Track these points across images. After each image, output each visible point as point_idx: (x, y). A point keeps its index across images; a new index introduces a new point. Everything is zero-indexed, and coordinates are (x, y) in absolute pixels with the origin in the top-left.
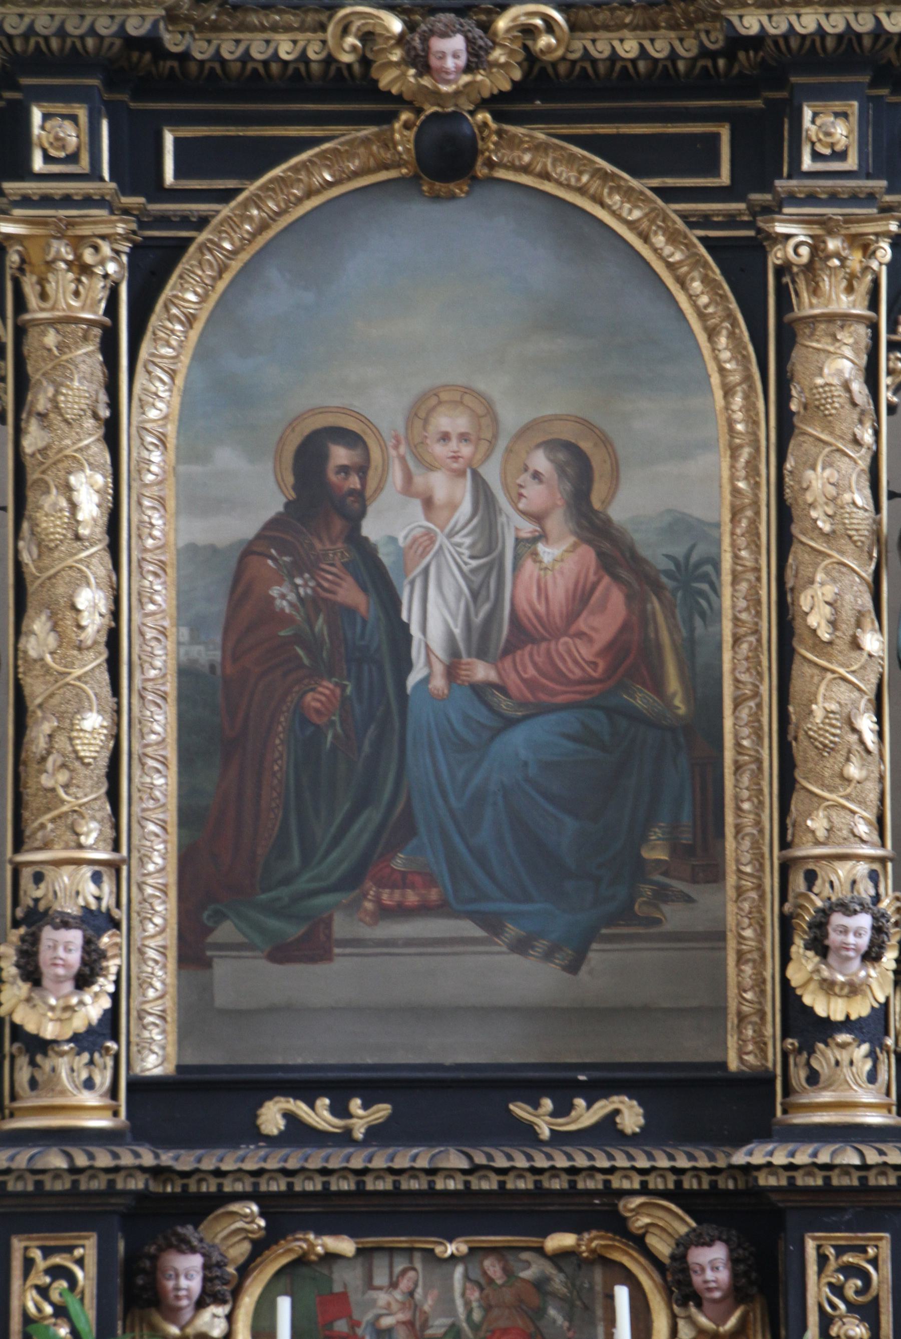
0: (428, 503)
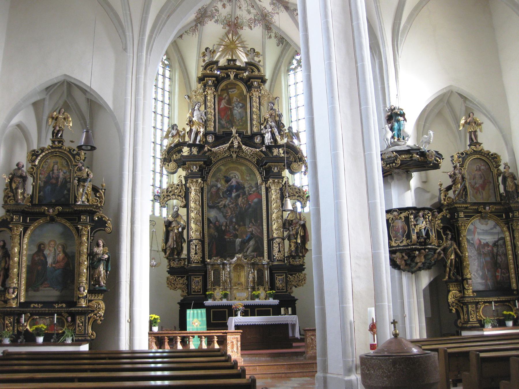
0: (50, 250)
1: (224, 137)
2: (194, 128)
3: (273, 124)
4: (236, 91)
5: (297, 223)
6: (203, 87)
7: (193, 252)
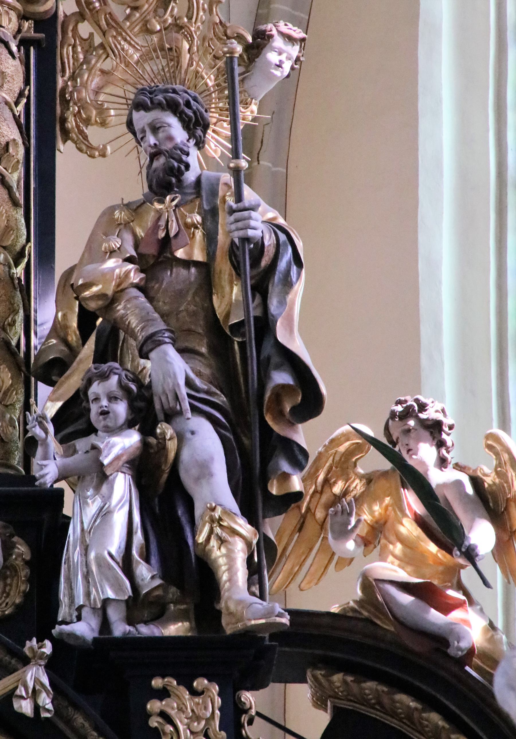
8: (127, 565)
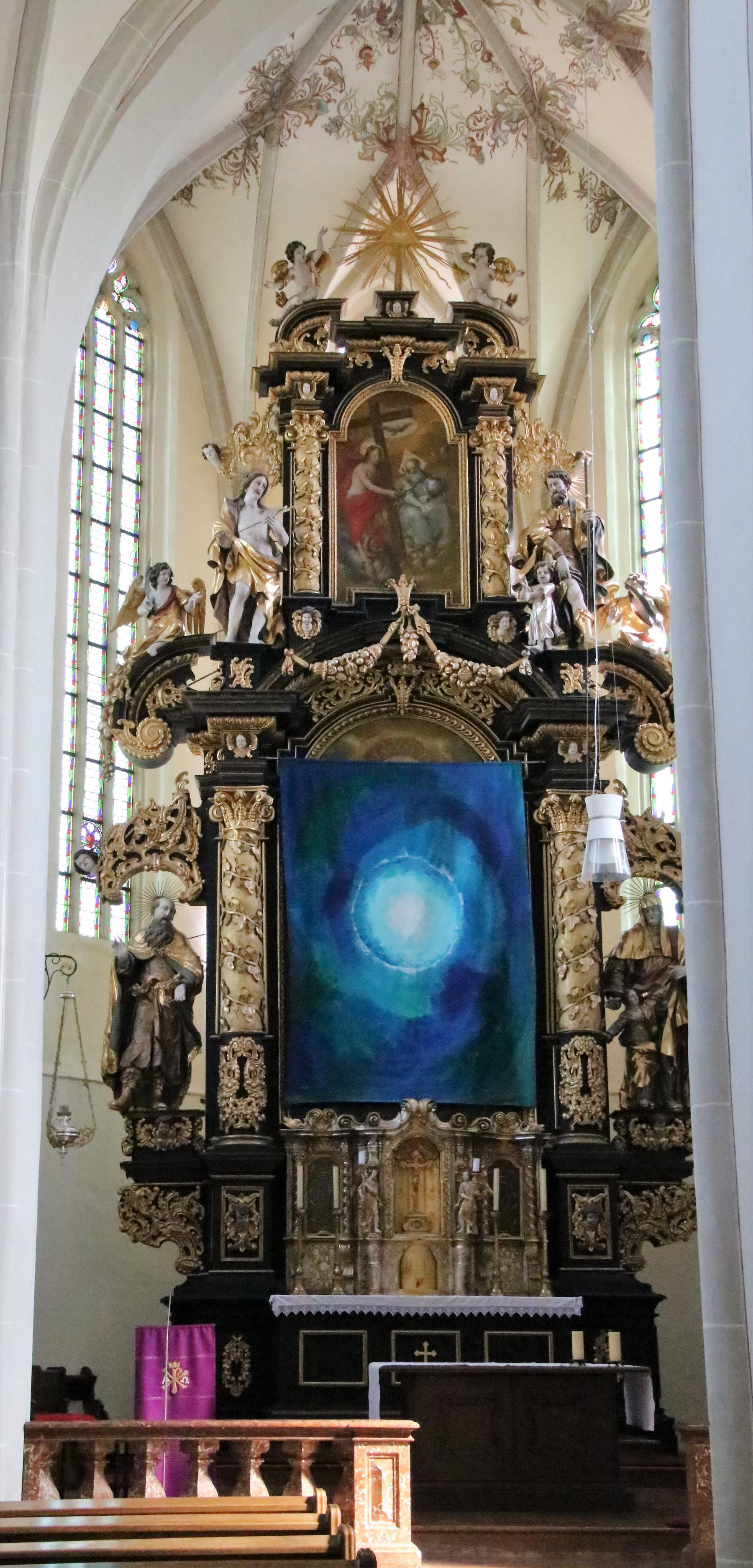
1: (362, 617)
2: (242, 582)
3: (566, 564)
4: (413, 428)
5: (661, 973)
6: (276, 409)
7: (229, 1085)
8: (552, 627)
